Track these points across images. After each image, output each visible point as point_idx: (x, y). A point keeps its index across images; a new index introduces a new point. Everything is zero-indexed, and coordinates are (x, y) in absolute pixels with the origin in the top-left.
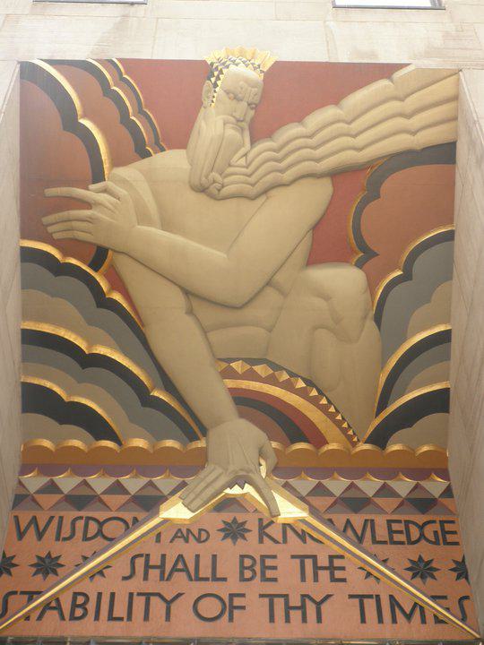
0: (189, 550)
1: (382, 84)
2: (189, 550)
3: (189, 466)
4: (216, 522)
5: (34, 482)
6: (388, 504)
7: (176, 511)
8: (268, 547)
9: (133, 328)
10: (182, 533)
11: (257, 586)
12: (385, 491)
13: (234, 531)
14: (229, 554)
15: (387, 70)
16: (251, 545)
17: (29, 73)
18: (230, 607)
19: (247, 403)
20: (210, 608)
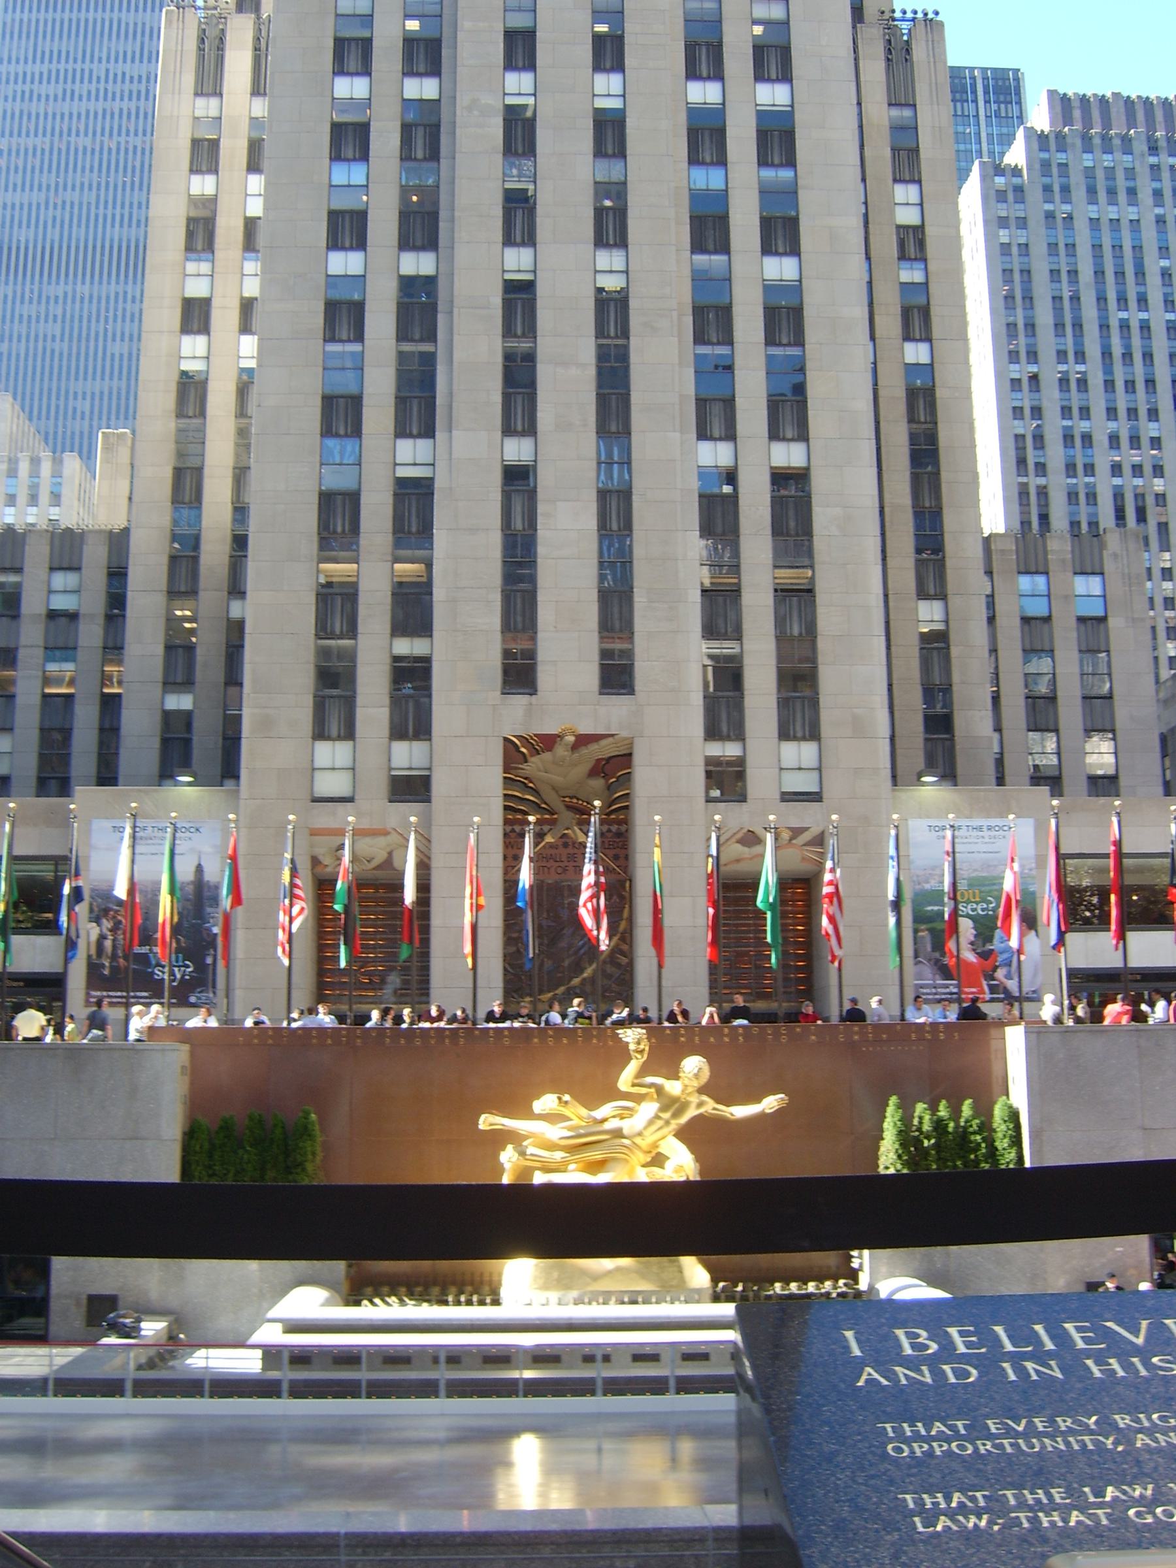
0: (553, 851)
1: (611, 739)
2: (553, 851)
3: (553, 822)
4: (560, 843)
5: (509, 828)
6: (609, 835)
7: (549, 839)
8: (576, 851)
9: (535, 792)
10: (551, 846)
11: (572, 864)
12: (609, 831)
13: (566, 845)
14: (564, 852)
15: (612, 735)
16: (570, 850)
17: (506, 739)
18: (565, 870)
19: (569, 807)
20: (559, 870)
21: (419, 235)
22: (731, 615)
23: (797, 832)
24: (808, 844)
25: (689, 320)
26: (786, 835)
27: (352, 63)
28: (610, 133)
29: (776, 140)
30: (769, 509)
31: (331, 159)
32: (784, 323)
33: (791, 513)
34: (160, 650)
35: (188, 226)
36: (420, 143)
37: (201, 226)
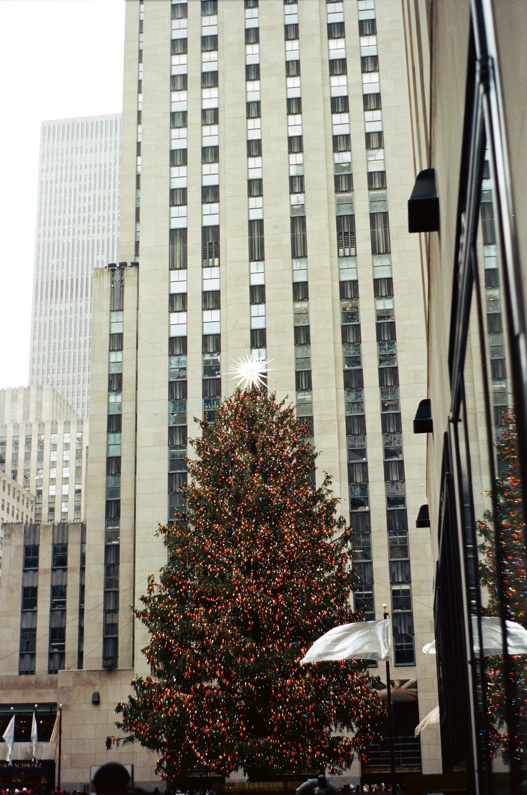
21: (212, 390)
22: (368, 573)
23: (403, 682)
24: (409, 687)
25: (343, 424)
26: (397, 684)
27: (178, 306)
28: (302, 333)
29: (386, 328)
30: (386, 517)
31: (169, 355)
32: (391, 422)
33: (397, 518)
34: (102, 593)
35: (109, 378)
36: (211, 344)
37: (115, 377)
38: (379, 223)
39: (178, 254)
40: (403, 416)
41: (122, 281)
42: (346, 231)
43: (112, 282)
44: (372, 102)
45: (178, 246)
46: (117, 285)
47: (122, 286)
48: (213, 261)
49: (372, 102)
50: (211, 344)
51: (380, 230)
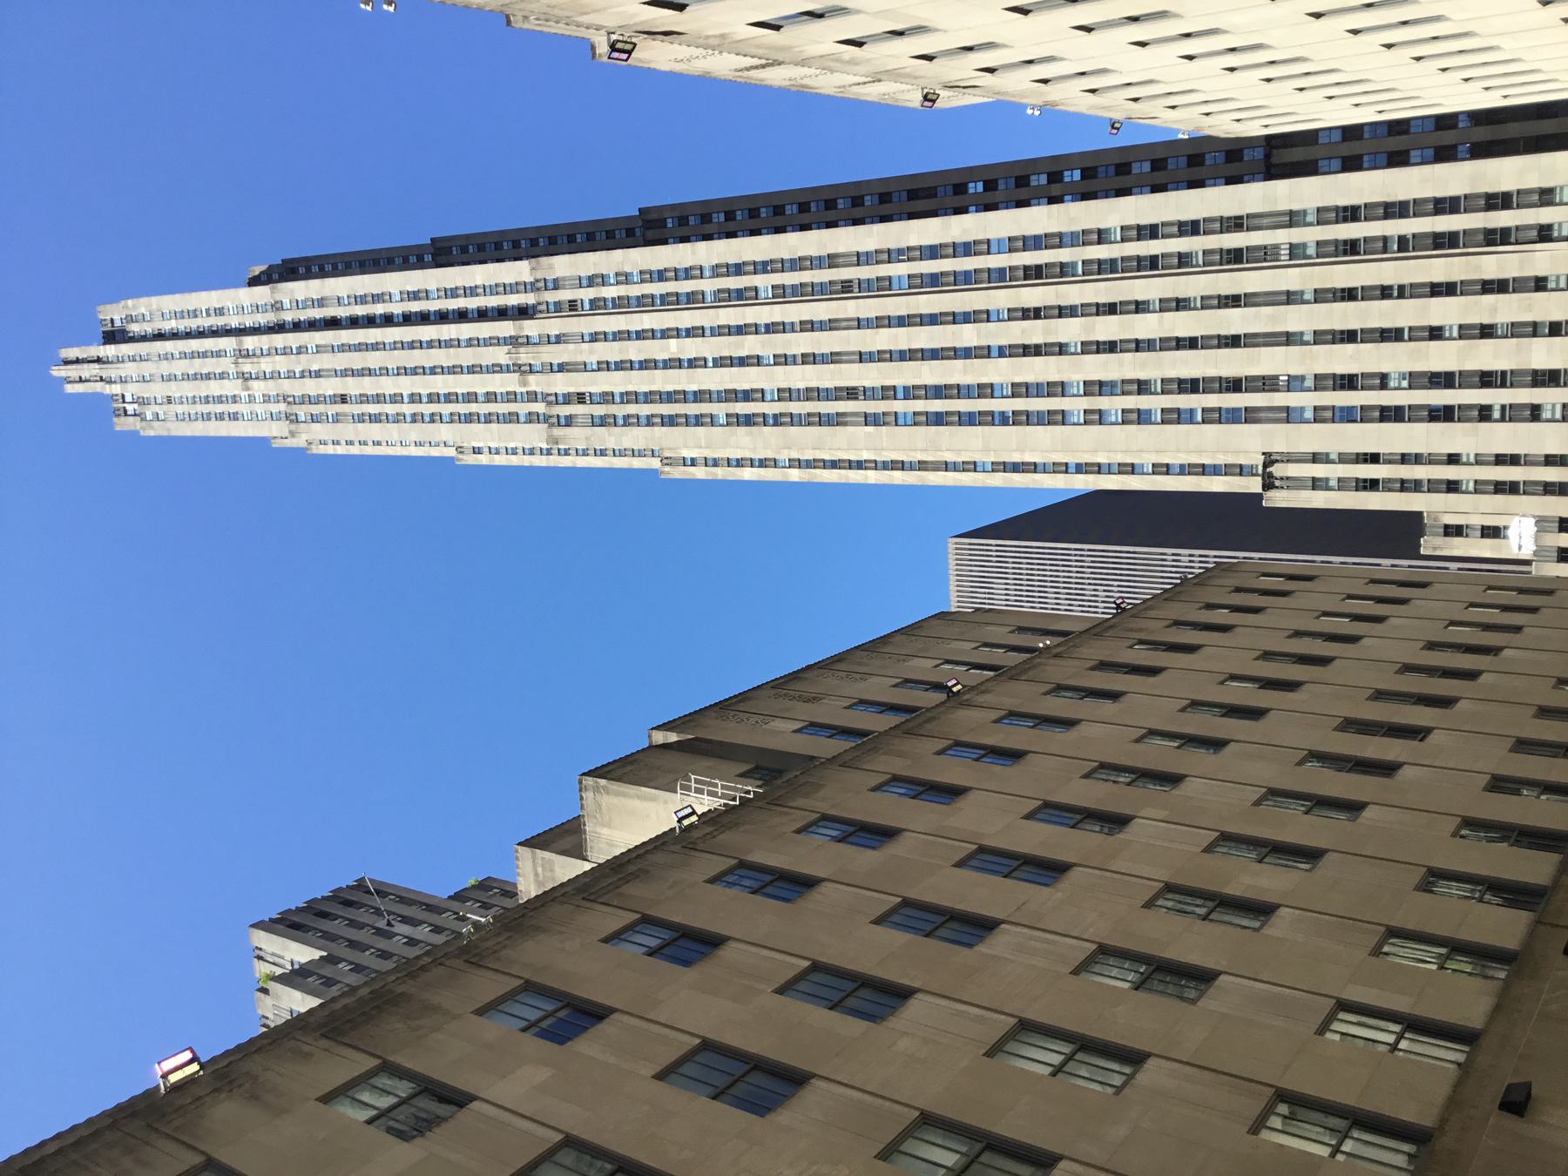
27: (1329, 414)
32: (1473, 203)
38: (1257, 222)
39: (1271, 415)
40: (1468, 191)
41: (1282, 479)
42: (1263, 254)
43: (1282, 488)
44: (1129, 233)
45: (1263, 415)
46: (1284, 483)
47: (1288, 478)
48: (1282, 381)
49: (1129, 233)
50: (1371, 382)
51: (1265, 221)
